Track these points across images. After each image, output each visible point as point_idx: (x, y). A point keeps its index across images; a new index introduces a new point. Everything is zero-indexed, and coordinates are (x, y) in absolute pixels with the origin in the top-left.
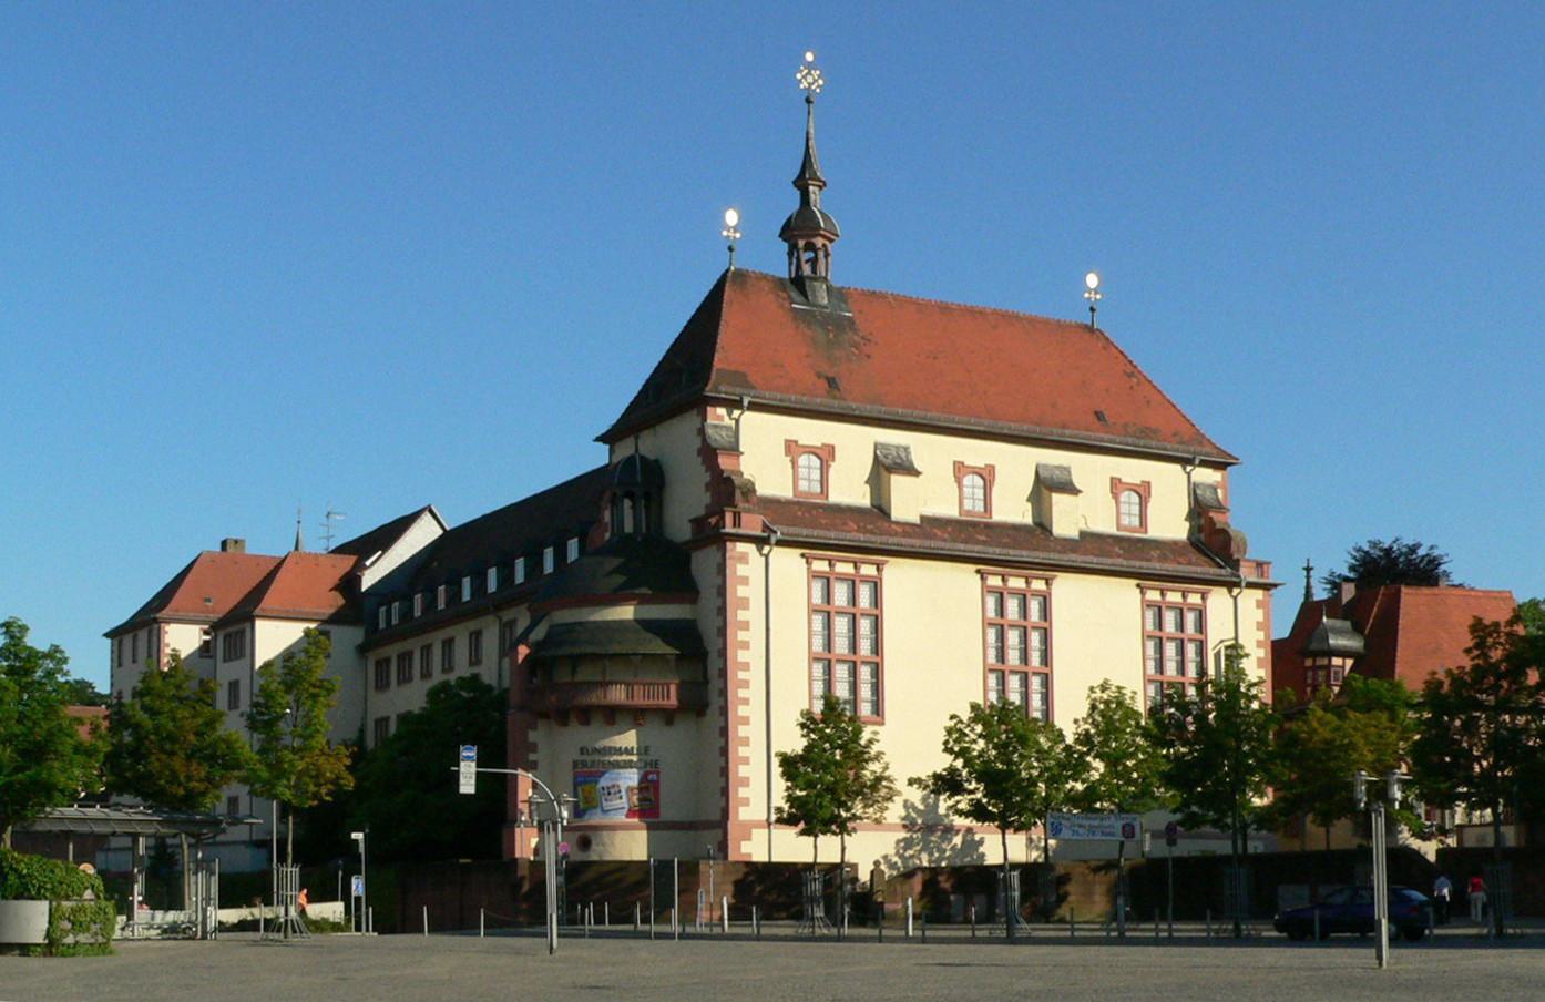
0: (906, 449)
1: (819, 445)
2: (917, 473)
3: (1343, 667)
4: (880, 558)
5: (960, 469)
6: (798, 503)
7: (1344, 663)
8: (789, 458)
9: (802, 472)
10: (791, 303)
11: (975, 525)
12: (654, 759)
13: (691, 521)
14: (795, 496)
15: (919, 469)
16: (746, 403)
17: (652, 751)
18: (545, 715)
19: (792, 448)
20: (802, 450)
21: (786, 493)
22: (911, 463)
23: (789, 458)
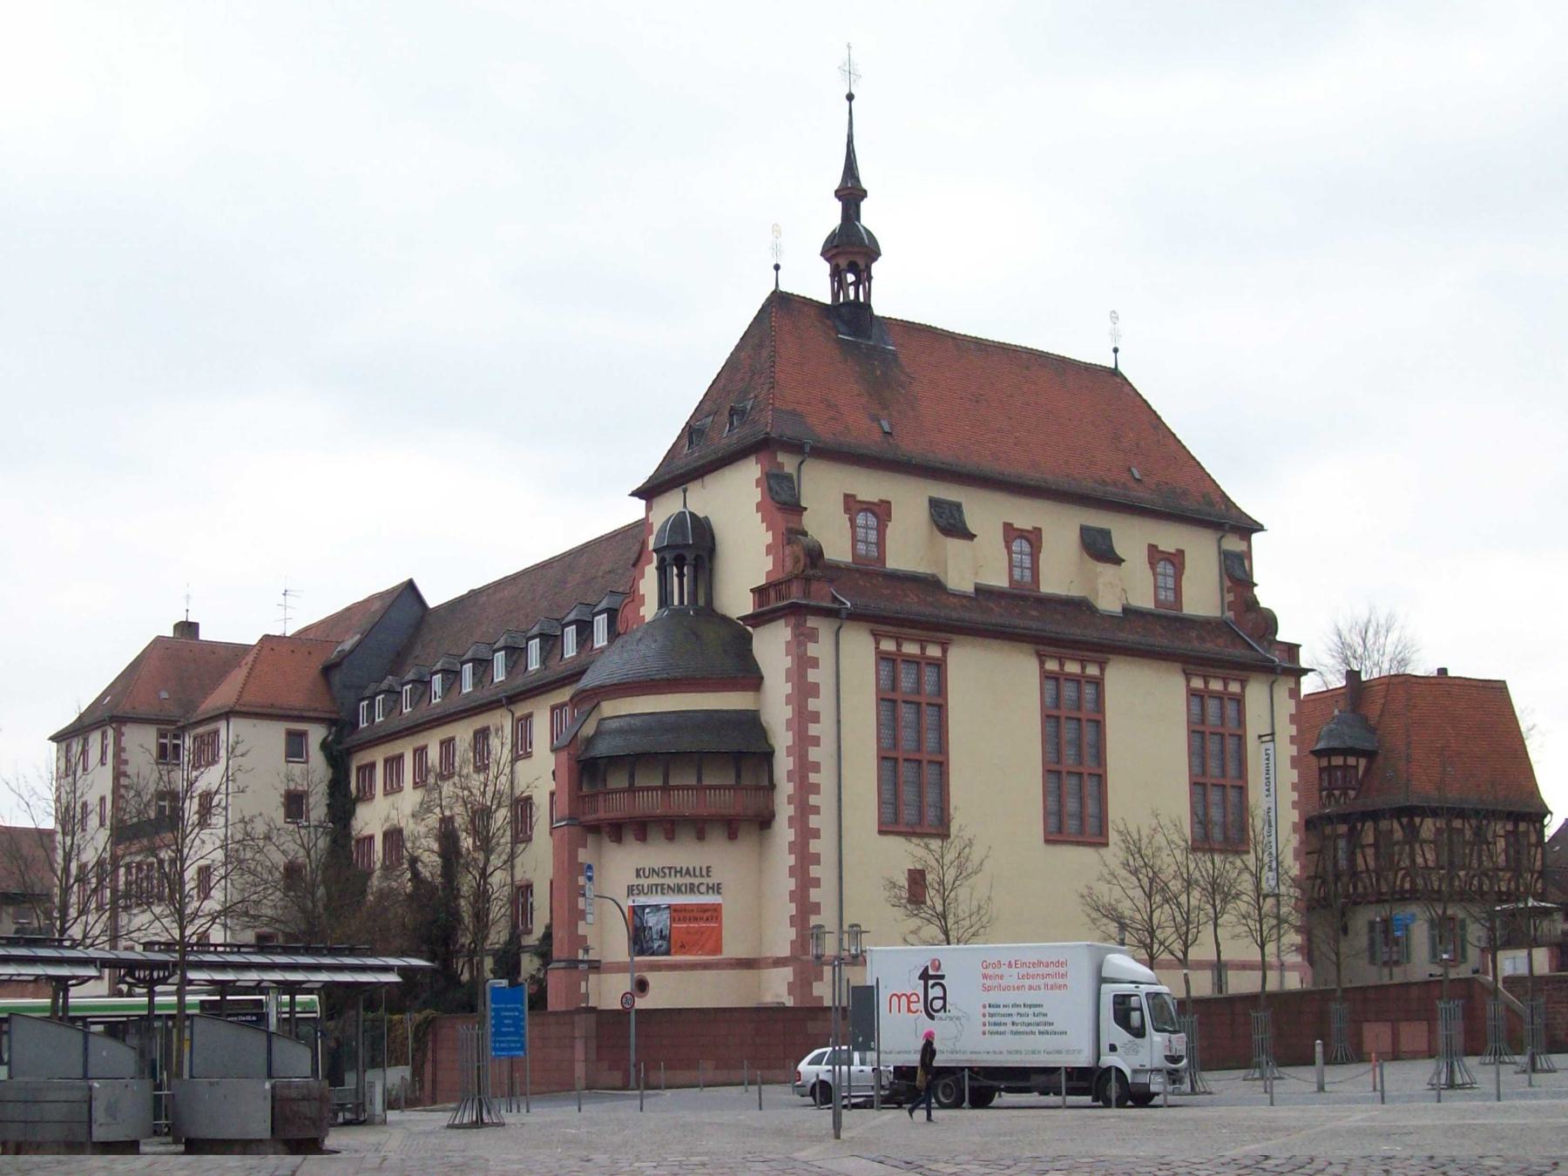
0: (958, 506)
1: (876, 500)
2: (972, 537)
3: (1356, 767)
4: (943, 635)
5: (1011, 533)
6: (858, 570)
7: (1357, 761)
8: (847, 516)
9: (861, 532)
10: (837, 334)
11: (1023, 598)
12: (716, 882)
13: (752, 590)
14: (853, 562)
15: (974, 532)
16: (807, 449)
17: (713, 871)
18: (594, 829)
19: (852, 504)
20: (859, 506)
21: (846, 558)
22: (967, 529)
23: (847, 516)
